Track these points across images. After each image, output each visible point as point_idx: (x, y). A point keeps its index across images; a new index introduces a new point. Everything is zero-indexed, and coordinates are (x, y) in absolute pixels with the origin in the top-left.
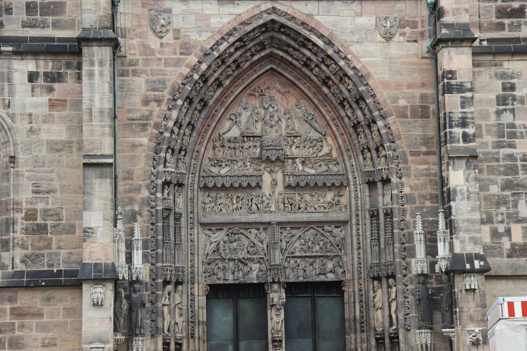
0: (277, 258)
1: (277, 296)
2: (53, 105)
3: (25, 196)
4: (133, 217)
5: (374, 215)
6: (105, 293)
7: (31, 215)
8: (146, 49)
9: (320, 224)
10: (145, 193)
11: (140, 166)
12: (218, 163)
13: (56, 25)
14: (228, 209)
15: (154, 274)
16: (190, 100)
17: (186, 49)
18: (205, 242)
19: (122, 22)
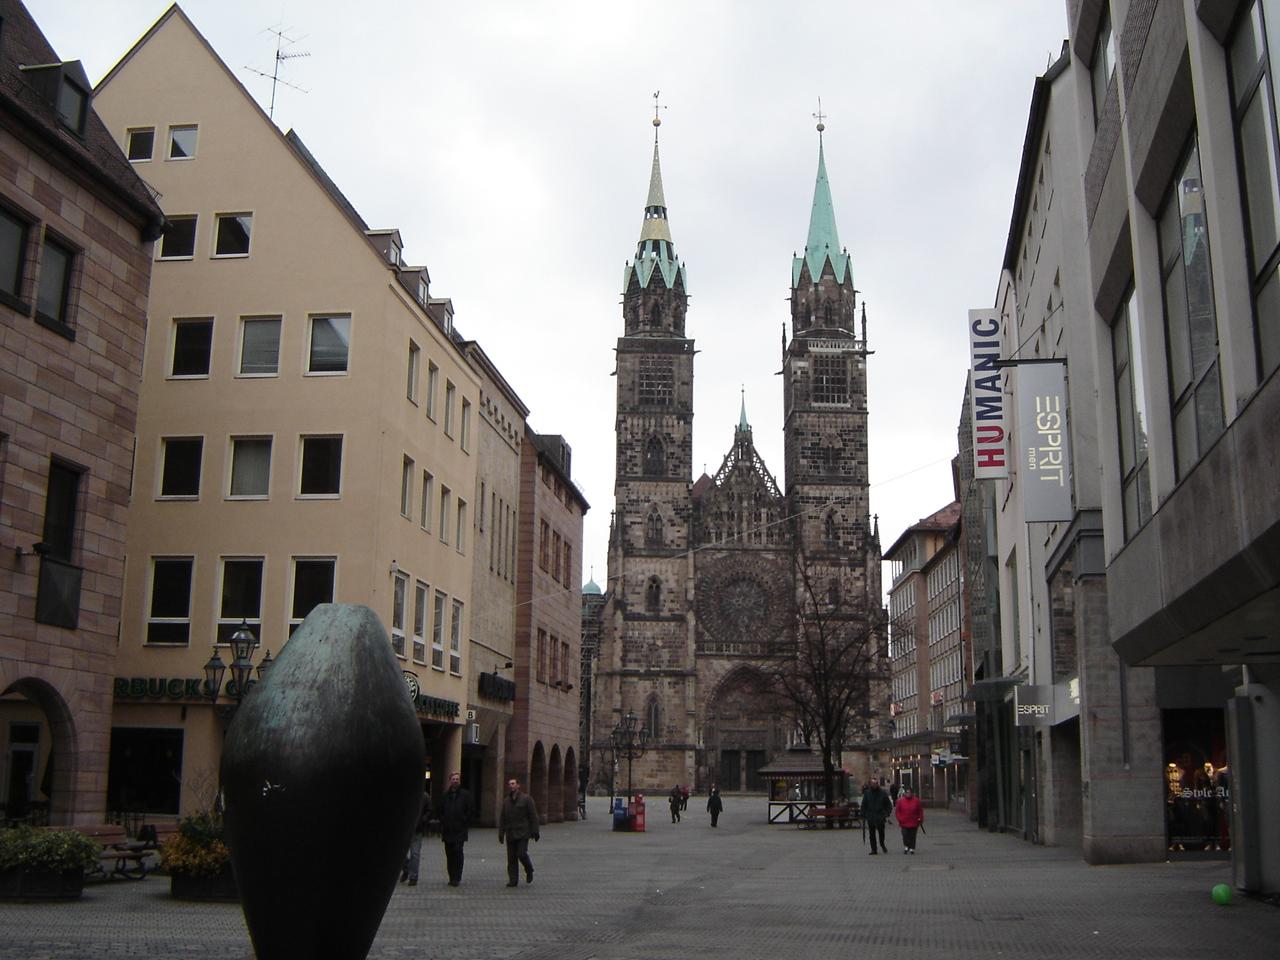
0: (744, 743)
1: (744, 755)
2: (676, 692)
3: (667, 721)
4: (700, 729)
5: (775, 730)
6: (692, 753)
7: (668, 727)
8: (705, 676)
9: (758, 732)
10: (703, 722)
11: (702, 713)
12: (725, 710)
13: (677, 667)
14: (728, 726)
15: (706, 747)
16: (717, 691)
17: (717, 675)
18: (721, 736)
19: (698, 667)
